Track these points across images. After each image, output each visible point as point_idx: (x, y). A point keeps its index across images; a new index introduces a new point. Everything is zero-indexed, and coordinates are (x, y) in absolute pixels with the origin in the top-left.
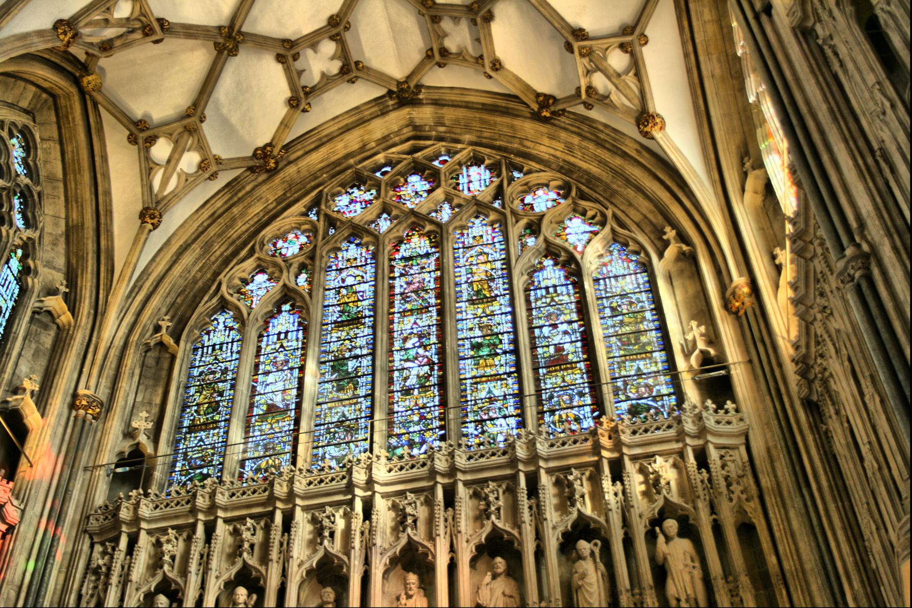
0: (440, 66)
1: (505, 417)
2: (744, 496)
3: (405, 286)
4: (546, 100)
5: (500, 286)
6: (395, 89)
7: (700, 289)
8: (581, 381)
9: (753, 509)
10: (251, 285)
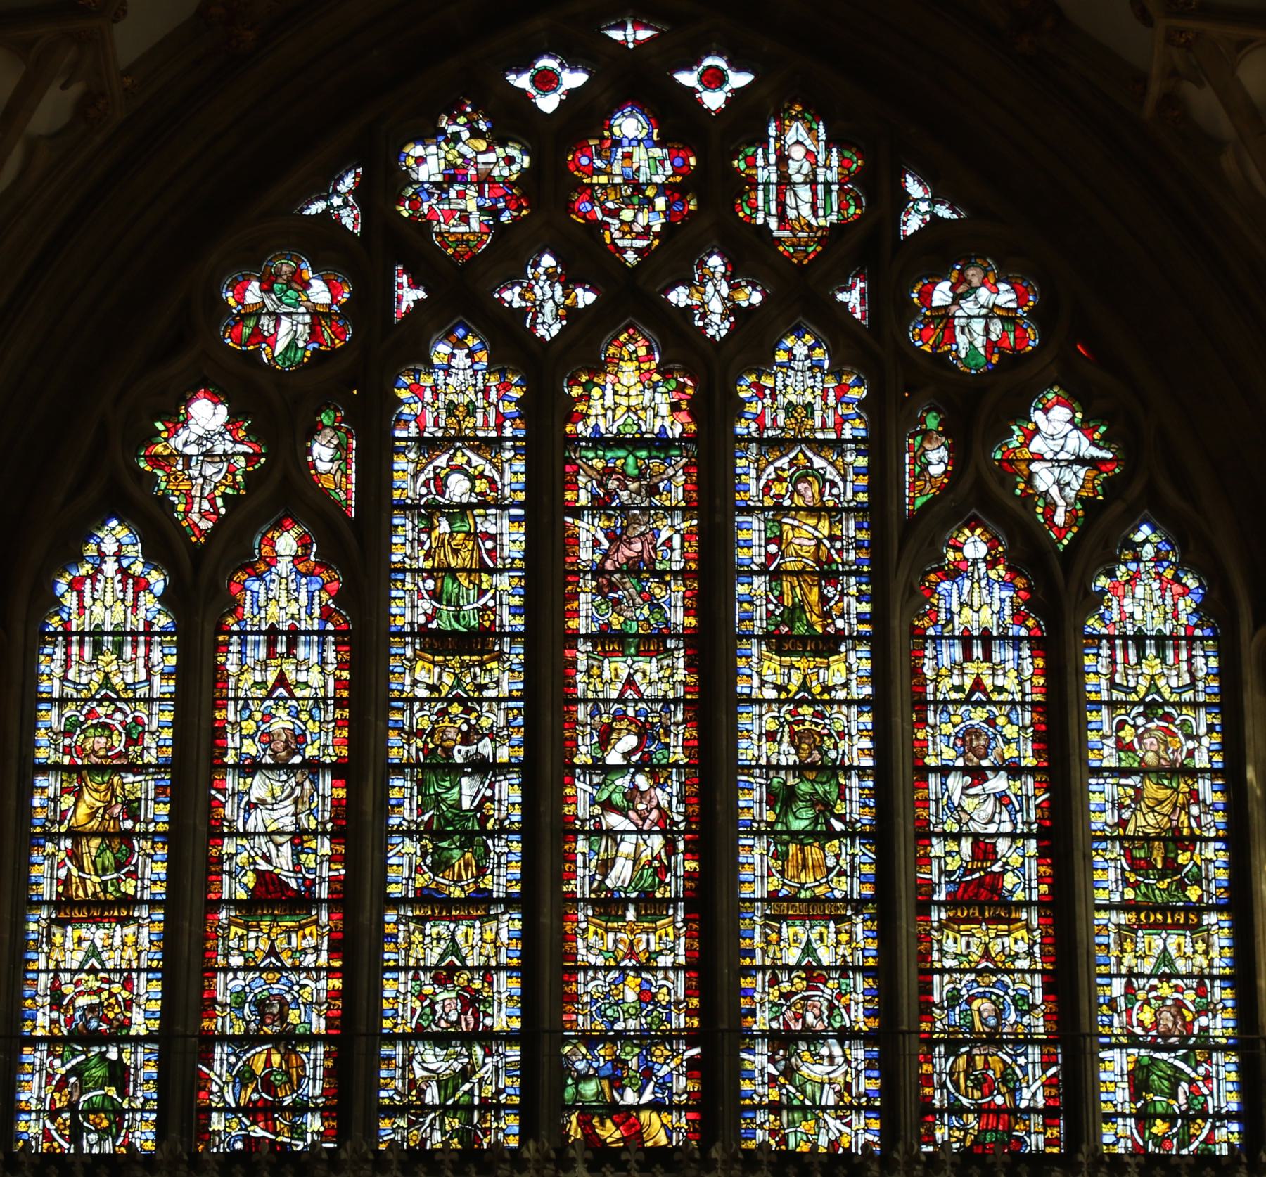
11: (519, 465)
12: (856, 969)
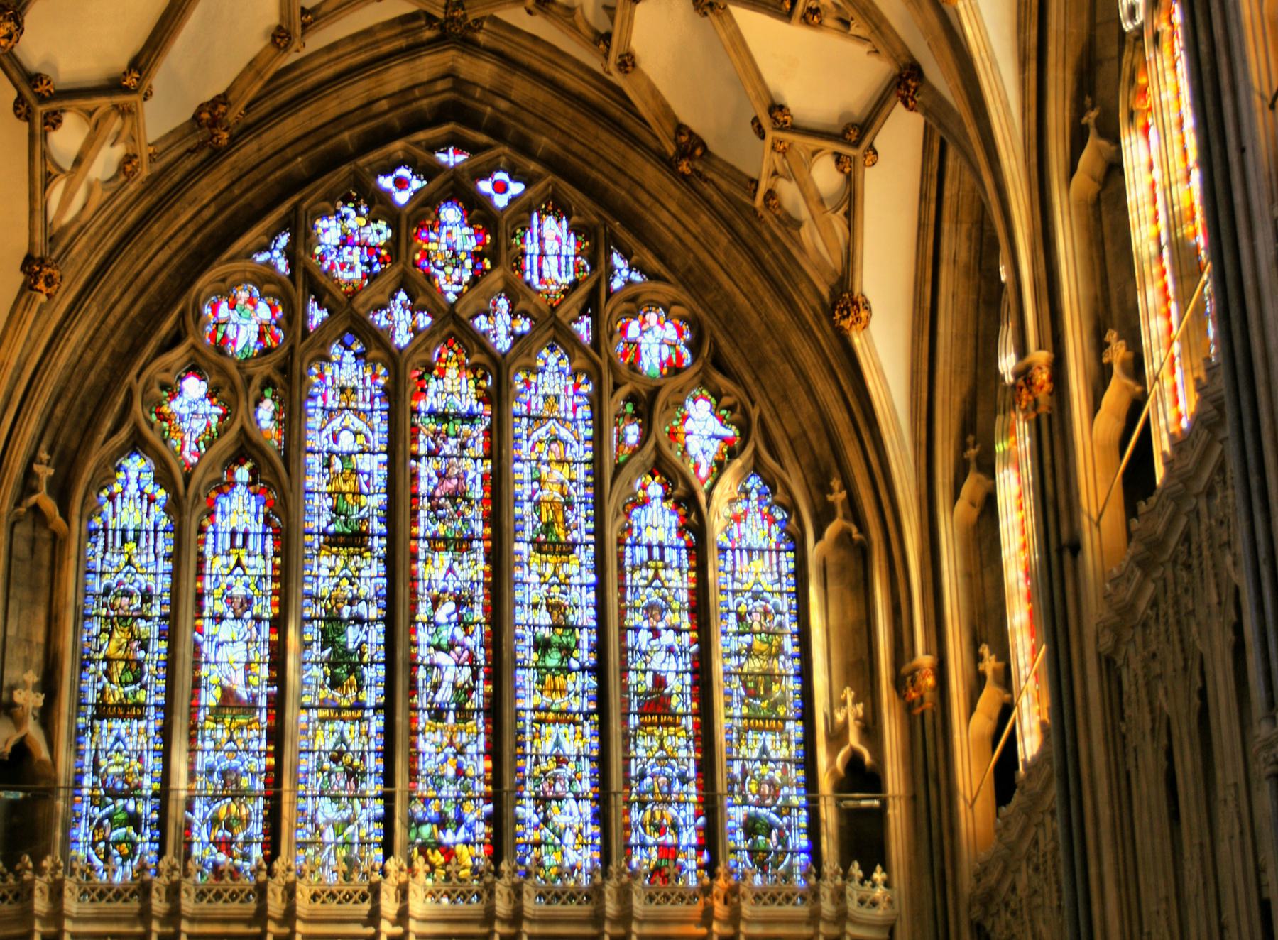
5: (581, 518)
7: (864, 617)
10: (179, 400)
11: (384, 427)
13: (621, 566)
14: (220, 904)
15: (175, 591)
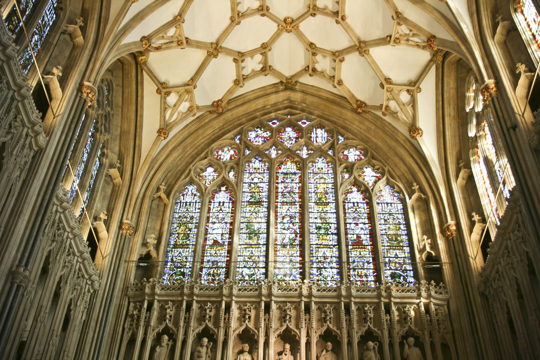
0: (310, 75)
1: (331, 268)
2: (445, 331)
3: (284, 188)
4: (361, 104)
5: (331, 198)
6: (284, 81)
7: (428, 218)
8: (368, 256)
9: (449, 338)
10: (205, 172)
11: (268, 177)
12: (334, 257)
13: (344, 208)
14: (207, 291)
15: (200, 217)
